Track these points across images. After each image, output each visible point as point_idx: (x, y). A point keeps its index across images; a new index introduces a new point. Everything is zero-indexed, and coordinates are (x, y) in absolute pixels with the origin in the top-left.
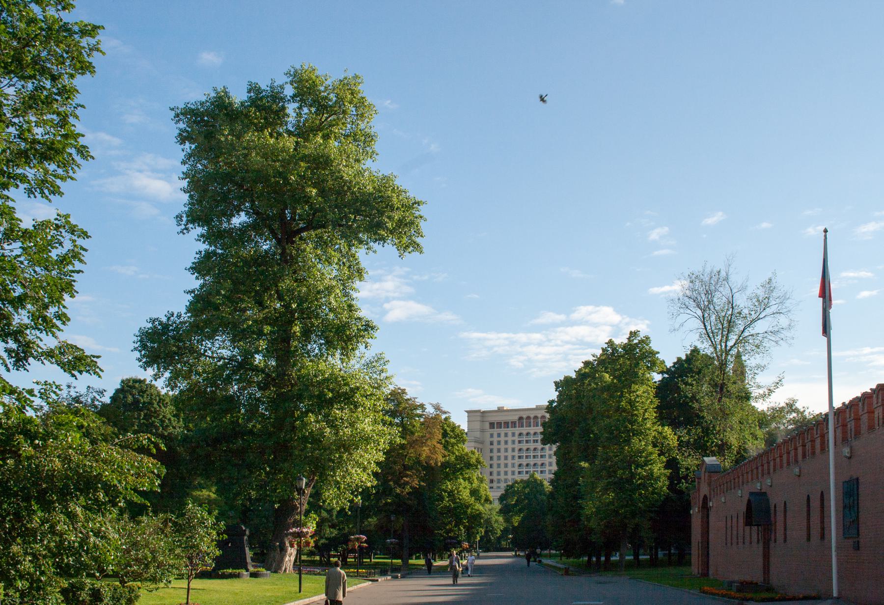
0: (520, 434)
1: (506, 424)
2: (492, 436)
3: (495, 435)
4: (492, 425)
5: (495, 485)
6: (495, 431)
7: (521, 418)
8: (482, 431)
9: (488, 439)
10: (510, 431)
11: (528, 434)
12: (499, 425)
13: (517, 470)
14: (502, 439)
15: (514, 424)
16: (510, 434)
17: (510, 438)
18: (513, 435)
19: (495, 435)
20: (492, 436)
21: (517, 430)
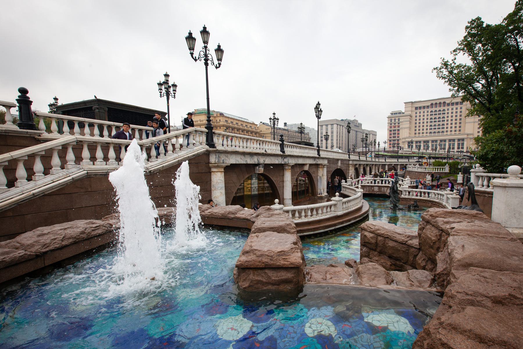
0: (431, 111)
1: (424, 107)
2: (416, 113)
3: (418, 113)
4: (416, 108)
5: (417, 135)
6: (418, 111)
7: (432, 104)
8: (412, 111)
9: (414, 115)
10: (426, 110)
11: (436, 111)
12: (420, 108)
13: (429, 128)
14: (422, 114)
15: (428, 107)
16: (426, 112)
17: (426, 114)
18: (428, 112)
19: (418, 113)
20: (416, 113)
21: (430, 110)
